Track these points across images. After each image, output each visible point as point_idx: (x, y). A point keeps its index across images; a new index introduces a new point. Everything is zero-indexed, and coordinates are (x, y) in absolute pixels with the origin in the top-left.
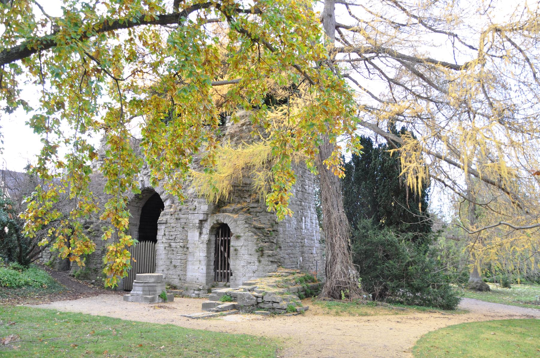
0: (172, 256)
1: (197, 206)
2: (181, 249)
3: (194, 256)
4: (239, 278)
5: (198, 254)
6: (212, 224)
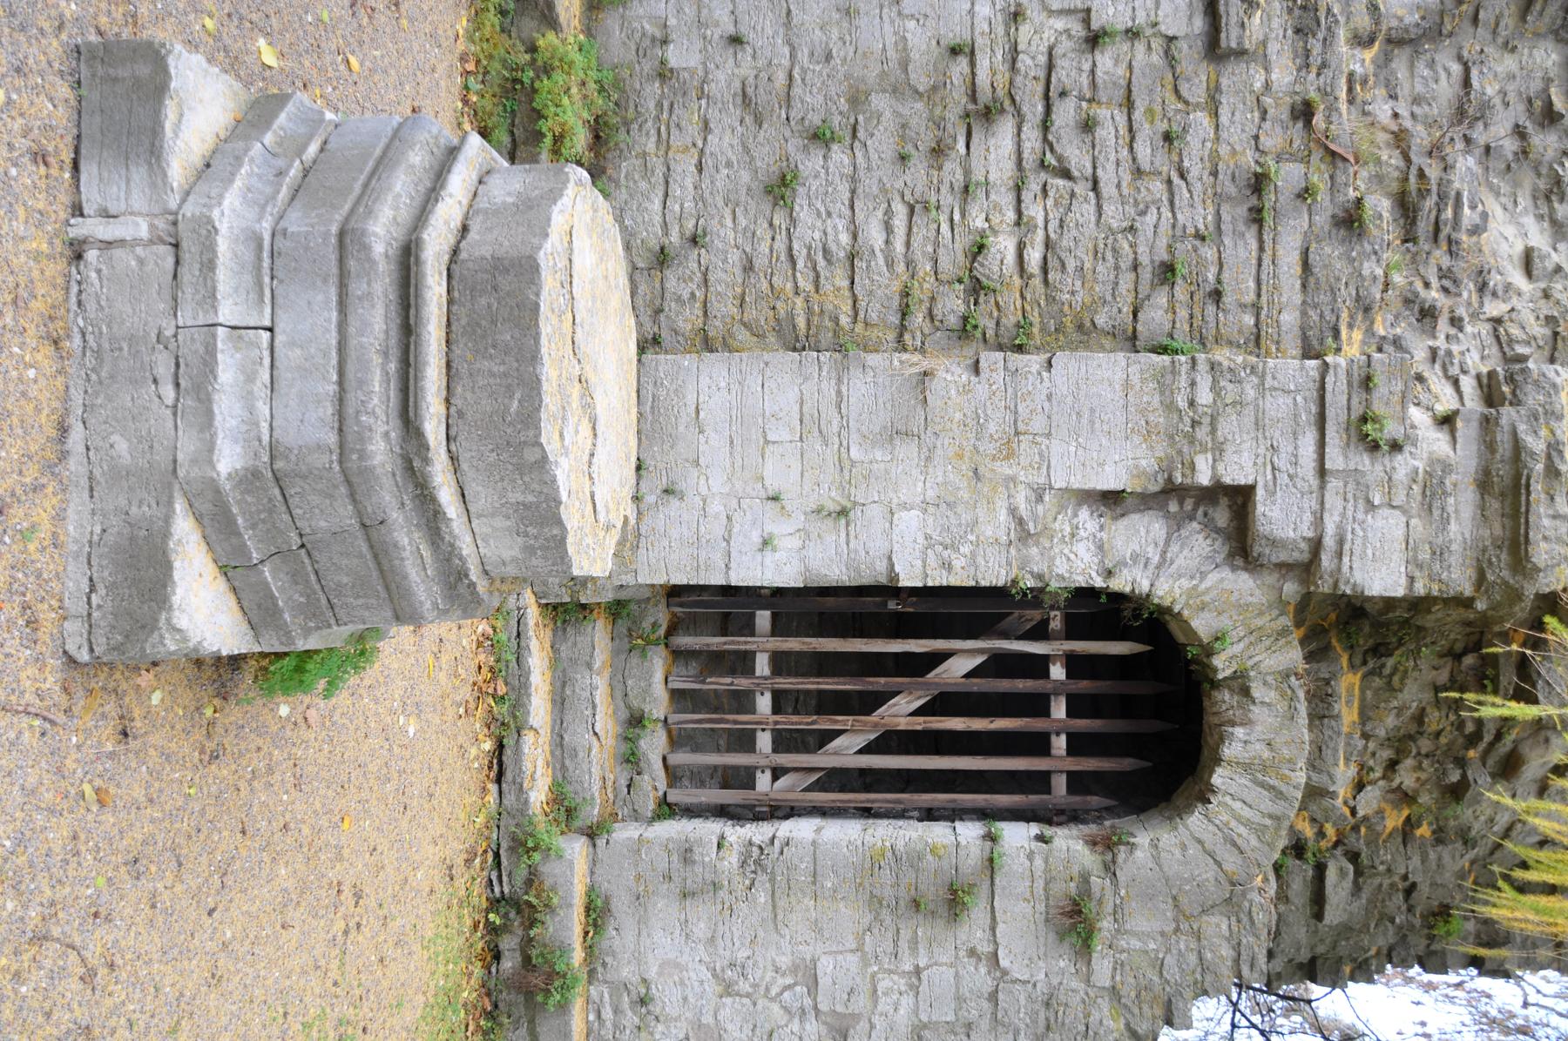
0: (882, 143)
1: (1403, 465)
2: (952, 260)
3: (896, 433)
4: (701, 929)
5: (913, 487)
6: (1202, 625)
